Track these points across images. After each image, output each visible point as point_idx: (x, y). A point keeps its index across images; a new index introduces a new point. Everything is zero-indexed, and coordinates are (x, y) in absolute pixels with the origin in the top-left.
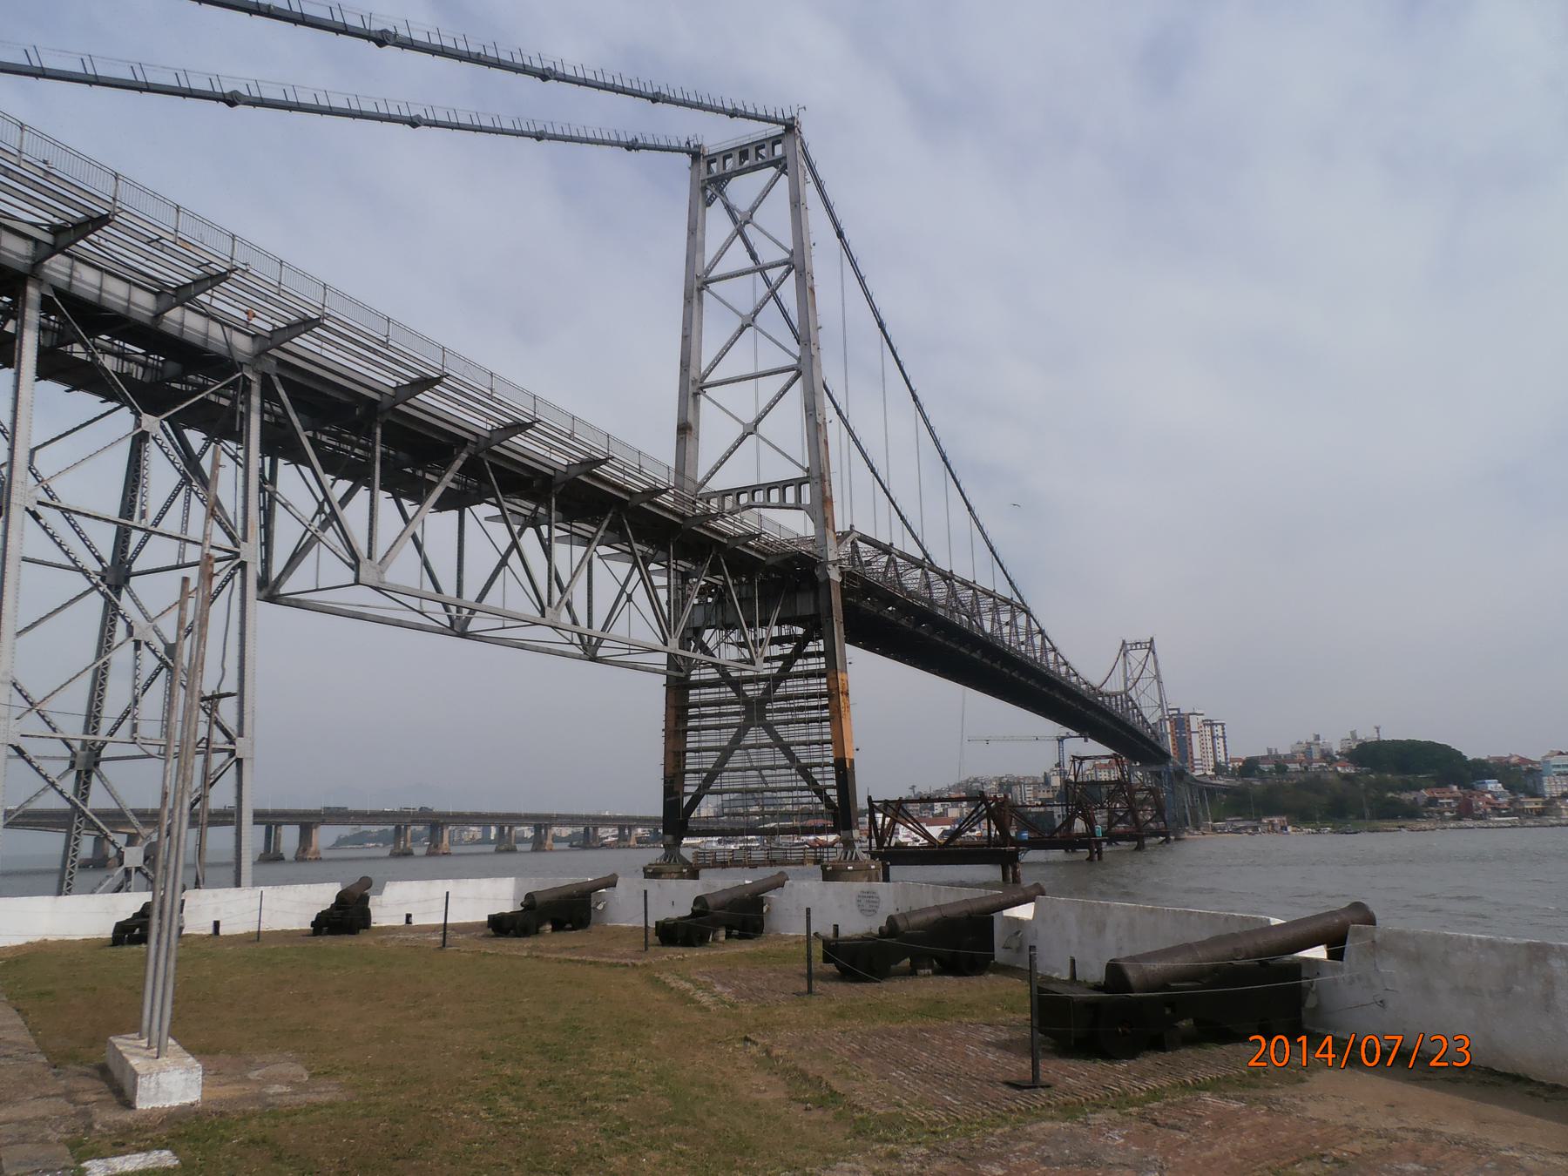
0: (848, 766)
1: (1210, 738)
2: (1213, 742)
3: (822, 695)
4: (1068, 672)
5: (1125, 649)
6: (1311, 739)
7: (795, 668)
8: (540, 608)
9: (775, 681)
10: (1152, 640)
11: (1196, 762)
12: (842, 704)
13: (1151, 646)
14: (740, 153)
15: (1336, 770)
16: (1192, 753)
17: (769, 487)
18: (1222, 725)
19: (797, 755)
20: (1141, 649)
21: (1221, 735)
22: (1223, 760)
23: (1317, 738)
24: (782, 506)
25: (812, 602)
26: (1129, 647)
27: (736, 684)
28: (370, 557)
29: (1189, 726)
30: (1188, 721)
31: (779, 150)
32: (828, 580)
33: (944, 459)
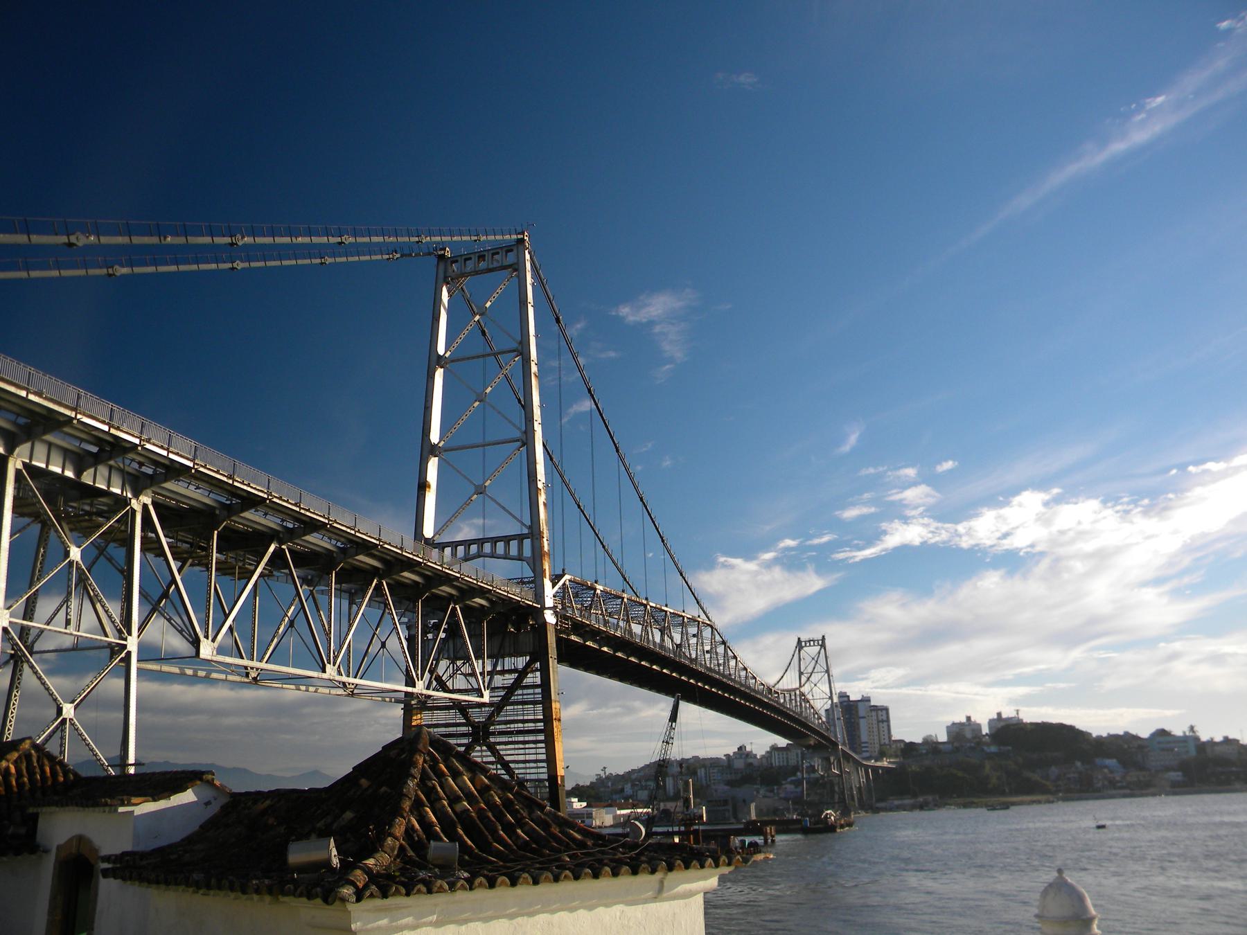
0: (559, 782)
1: (876, 722)
2: (878, 725)
3: (539, 721)
4: (746, 677)
5: (800, 645)
6: (964, 720)
7: (516, 698)
8: (321, 665)
9: (498, 707)
10: (823, 636)
11: (863, 745)
12: (555, 730)
13: (822, 643)
14: (479, 257)
15: (983, 750)
16: (859, 737)
17: (494, 541)
19: (517, 771)
20: (814, 645)
21: (884, 718)
22: (887, 742)
23: (969, 718)
24: (506, 557)
25: (531, 640)
26: (803, 644)
27: (462, 708)
28: (207, 637)
29: (857, 712)
30: (857, 707)
31: (511, 258)
32: (545, 623)
33: (641, 499)
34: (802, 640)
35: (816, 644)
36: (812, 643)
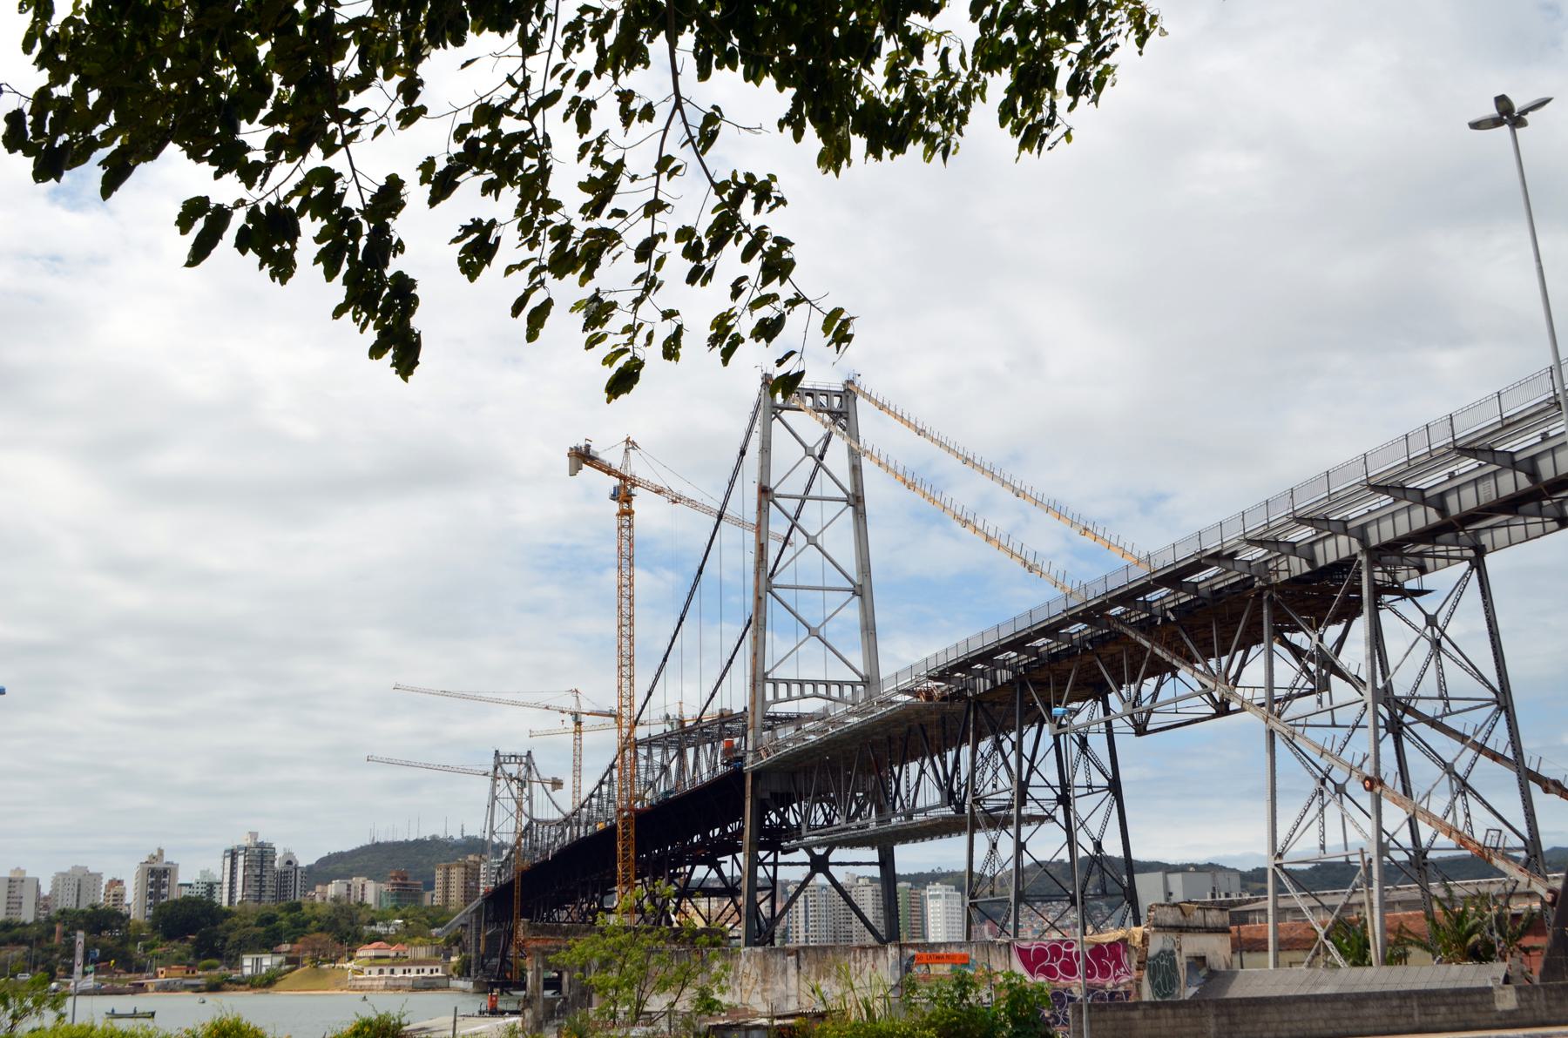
10: (529, 752)
17: (827, 684)
26: (502, 759)
34: (501, 753)
35: (518, 761)
36: (513, 759)
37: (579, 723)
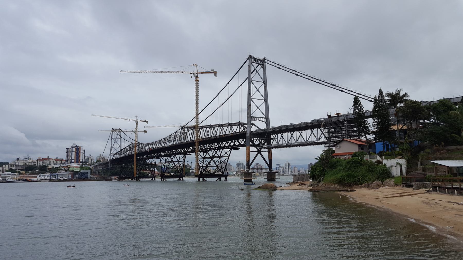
6: (89, 156)
11: (81, 161)
17: (260, 118)
18: (85, 150)
36: (116, 130)
37: (137, 123)
